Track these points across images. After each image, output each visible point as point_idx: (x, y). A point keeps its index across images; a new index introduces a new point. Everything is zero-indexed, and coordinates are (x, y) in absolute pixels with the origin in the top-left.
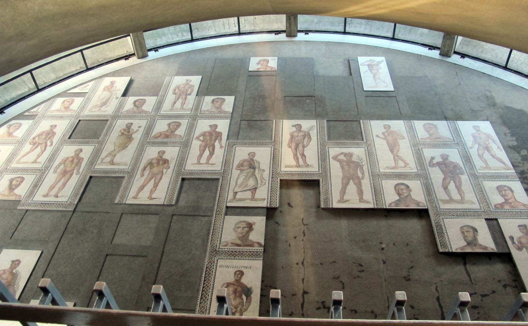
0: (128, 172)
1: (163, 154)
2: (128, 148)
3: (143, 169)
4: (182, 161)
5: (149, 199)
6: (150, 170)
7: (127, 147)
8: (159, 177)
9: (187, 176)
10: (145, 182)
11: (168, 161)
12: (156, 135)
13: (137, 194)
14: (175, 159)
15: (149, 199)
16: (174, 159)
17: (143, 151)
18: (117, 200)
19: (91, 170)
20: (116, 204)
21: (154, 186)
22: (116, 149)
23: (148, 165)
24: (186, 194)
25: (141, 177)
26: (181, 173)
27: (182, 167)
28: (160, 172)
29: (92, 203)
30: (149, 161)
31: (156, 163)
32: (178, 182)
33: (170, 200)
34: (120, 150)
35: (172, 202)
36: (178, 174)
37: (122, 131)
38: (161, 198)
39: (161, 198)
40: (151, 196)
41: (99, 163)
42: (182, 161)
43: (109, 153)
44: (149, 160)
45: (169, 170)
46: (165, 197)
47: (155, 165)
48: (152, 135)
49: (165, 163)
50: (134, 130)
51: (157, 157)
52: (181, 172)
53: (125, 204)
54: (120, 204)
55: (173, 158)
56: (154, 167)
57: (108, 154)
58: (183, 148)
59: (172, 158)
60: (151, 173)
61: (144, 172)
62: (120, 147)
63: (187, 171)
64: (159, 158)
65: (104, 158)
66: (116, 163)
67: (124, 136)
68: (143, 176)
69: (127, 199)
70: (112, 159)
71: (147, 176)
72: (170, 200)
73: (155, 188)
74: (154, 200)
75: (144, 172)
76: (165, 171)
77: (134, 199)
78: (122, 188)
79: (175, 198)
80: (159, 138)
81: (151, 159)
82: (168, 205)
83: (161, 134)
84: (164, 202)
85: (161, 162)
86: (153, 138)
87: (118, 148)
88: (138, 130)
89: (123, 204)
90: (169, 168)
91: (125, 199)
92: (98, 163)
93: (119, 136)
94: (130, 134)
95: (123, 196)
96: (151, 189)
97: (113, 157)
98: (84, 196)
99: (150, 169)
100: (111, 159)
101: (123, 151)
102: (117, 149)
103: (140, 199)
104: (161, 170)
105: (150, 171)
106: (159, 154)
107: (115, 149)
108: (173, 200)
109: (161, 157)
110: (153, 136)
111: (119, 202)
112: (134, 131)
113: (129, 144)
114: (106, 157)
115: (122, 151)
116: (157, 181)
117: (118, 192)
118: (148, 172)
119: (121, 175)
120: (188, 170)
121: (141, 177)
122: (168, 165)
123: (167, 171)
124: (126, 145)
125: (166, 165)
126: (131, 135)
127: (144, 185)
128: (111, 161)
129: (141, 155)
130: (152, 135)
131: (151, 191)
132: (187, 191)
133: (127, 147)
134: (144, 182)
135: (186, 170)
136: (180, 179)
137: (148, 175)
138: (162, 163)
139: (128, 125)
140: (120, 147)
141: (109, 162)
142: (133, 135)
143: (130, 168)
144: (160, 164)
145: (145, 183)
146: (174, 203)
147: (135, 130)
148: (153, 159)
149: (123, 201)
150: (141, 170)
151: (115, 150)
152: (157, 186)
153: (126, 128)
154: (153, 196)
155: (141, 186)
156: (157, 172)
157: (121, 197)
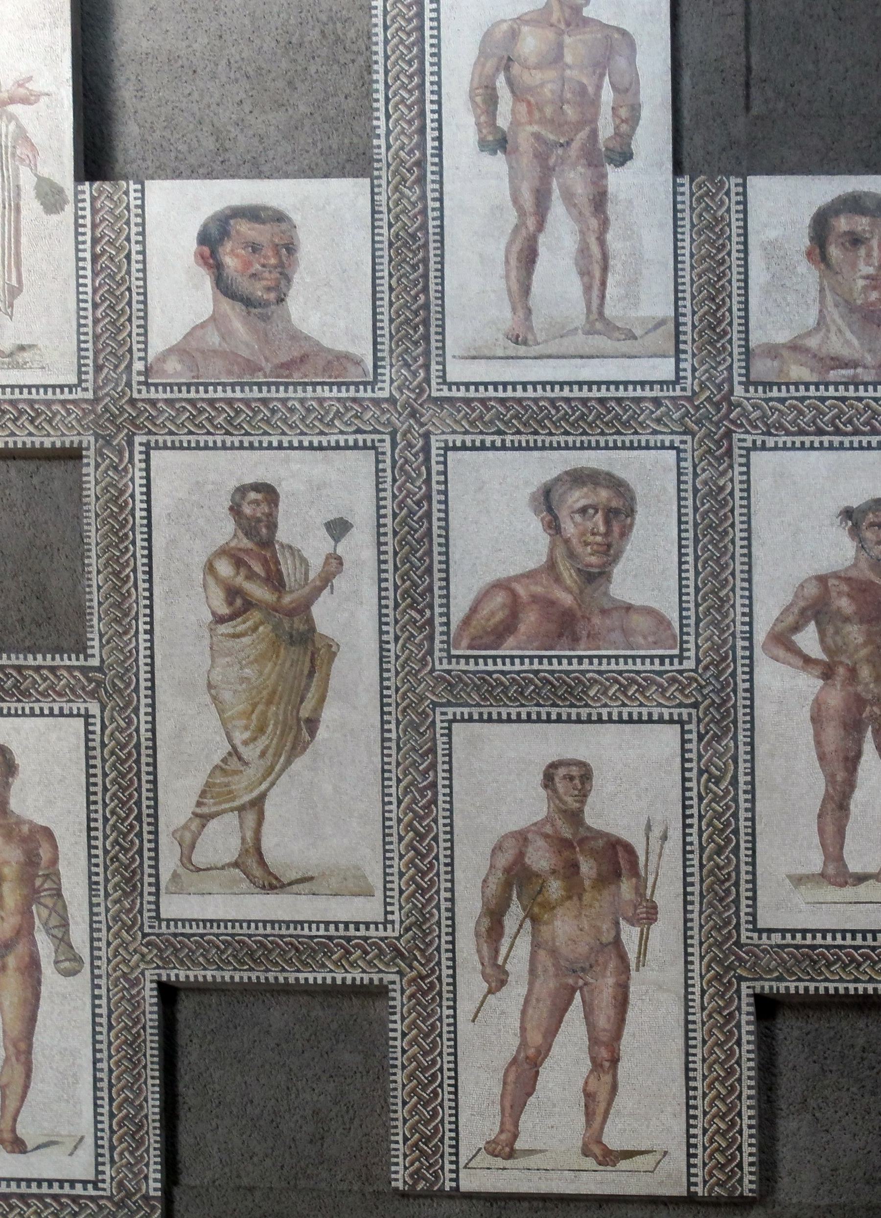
0: (400, 955)
1: (583, 796)
2: (322, 733)
3: (486, 922)
4: (719, 851)
5: (590, 1163)
6: (535, 934)
7: (312, 733)
8: (607, 984)
9: (780, 979)
10: (528, 1026)
11: (629, 850)
12: (485, 612)
13: (509, 1126)
14: (676, 834)
15: (596, 1158)
16: (664, 838)
17: (433, 766)
18: (400, 1168)
19: (145, 935)
20: (404, 1195)
21: (596, 1065)
22: (247, 753)
23: (507, 886)
24: (809, 1117)
25: (490, 992)
26: (739, 959)
27: (737, 901)
28: (603, 945)
29: (251, 1189)
30: (504, 860)
31: (554, 872)
32: (738, 1026)
33: (722, 1167)
34: (277, 755)
35: (740, 1181)
36: (720, 963)
37: (225, 568)
38: (666, 1153)
39: (666, 1153)
40: (599, 1142)
41: (175, 876)
42: (719, 851)
43: (207, 784)
44: (498, 849)
45: (656, 930)
46: (689, 1146)
47: (555, 888)
48: (457, 615)
49: (618, 874)
50: (304, 561)
51: (548, 820)
52: (737, 943)
53: (456, 1194)
54: (429, 1195)
55: (656, 833)
56: (549, 907)
57: (203, 794)
58: (700, 738)
59: (649, 828)
60: (542, 954)
61: (503, 951)
62: (261, 729)
63: (776, 938)
64: (567, 832)
65: (185, 827)
66: (294, 875)
67: (256, 616)
68: (503, 983)
69: (463, 1161)
70: (249, 834)
71: (531, 984)
72: (722, 1167)
73: (607, 1078)
74: (623, 1164)
75: (497, 951)
76: (630, 935)
77: (500, 1162)
78: (400, 1077)
79: (748, 1153)
80: (511, 641)
81: (514, 835)
82: (719, 1196)
83: (514, 595)
84: (690, 1184)
85: (587, 868)
86: (465, 643)
87: (254, 739)
88: (340, 561)
89: (442, 1194)
90: (651, 914)
91: (447, 1158)
92: (165, 877)
93: (220, 620)
94: (287, 599)
95: (428, 1140)
96: (581, 1084)
97: (250, 818)
98: (185, 1139)
99: (528, 924)
100: (243, 839)
101: (298, 764)
102: (245, 743)
103: (533, 1161)
104: (608, 937)
105: (536, 945)
106: (555, 791)
107: (237, 742)
108: (740, 1166)
109: (575, 817)
110: (467, 621)
111: (416, 1182)
112: (312, 575)
113: (322, 699)
114: (204, 819)
115: (288, 762)
116: (603, 1021)
117: (386, 1108)
118: (523, 947)
119: (354, 976)
120: (783, 932)
121: (490, 992)
122: (640, 891)
123: (644, 940)
124: (304, 713)
125: (626, 888)
126: (304, 608)
127: (531, 1052)
128: (244, 852)
129: (434, 801)
130: (457, 615)
131: (589, 1096)
132: (812, 1103)
133: (312, 724)
134: (523, 1029)
135: (770, 931)
136: (747, 1006)
137: (532, 971)
138: (593, 873)
139: (247, 510)
140: (261, 729)
141: (236, 865)
142: (317, 610)
143: (396, 917)
144: (587, 883)
145: (536, 1038)
146: (748, 1185)
147: (316, 563)
148: (522, 837)
149: (437, 1177)
150: (477, 935)
151: (235, 752)
152: (615, 1061)
153: (246, 543)
154: (613, 1139)
155: (514, 1061)
156: (583, 949)
157: (416, 1145)
